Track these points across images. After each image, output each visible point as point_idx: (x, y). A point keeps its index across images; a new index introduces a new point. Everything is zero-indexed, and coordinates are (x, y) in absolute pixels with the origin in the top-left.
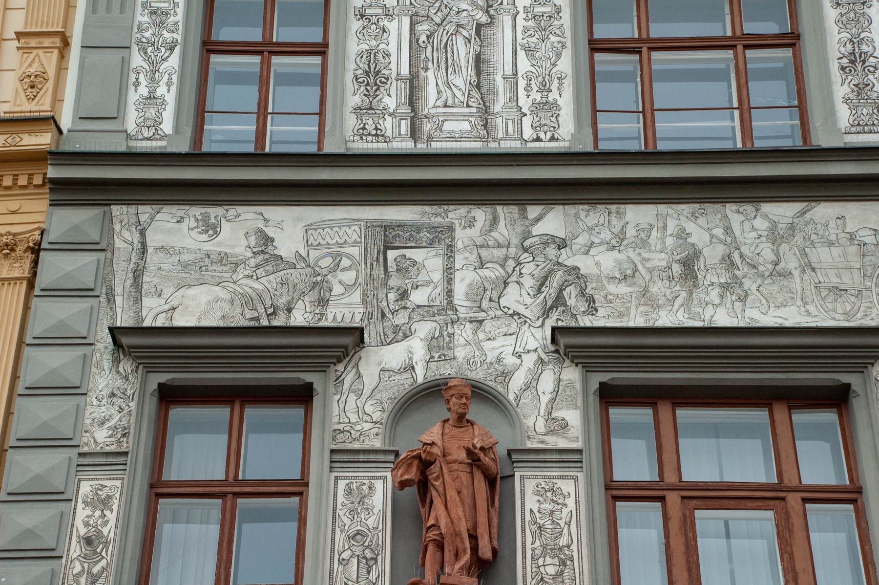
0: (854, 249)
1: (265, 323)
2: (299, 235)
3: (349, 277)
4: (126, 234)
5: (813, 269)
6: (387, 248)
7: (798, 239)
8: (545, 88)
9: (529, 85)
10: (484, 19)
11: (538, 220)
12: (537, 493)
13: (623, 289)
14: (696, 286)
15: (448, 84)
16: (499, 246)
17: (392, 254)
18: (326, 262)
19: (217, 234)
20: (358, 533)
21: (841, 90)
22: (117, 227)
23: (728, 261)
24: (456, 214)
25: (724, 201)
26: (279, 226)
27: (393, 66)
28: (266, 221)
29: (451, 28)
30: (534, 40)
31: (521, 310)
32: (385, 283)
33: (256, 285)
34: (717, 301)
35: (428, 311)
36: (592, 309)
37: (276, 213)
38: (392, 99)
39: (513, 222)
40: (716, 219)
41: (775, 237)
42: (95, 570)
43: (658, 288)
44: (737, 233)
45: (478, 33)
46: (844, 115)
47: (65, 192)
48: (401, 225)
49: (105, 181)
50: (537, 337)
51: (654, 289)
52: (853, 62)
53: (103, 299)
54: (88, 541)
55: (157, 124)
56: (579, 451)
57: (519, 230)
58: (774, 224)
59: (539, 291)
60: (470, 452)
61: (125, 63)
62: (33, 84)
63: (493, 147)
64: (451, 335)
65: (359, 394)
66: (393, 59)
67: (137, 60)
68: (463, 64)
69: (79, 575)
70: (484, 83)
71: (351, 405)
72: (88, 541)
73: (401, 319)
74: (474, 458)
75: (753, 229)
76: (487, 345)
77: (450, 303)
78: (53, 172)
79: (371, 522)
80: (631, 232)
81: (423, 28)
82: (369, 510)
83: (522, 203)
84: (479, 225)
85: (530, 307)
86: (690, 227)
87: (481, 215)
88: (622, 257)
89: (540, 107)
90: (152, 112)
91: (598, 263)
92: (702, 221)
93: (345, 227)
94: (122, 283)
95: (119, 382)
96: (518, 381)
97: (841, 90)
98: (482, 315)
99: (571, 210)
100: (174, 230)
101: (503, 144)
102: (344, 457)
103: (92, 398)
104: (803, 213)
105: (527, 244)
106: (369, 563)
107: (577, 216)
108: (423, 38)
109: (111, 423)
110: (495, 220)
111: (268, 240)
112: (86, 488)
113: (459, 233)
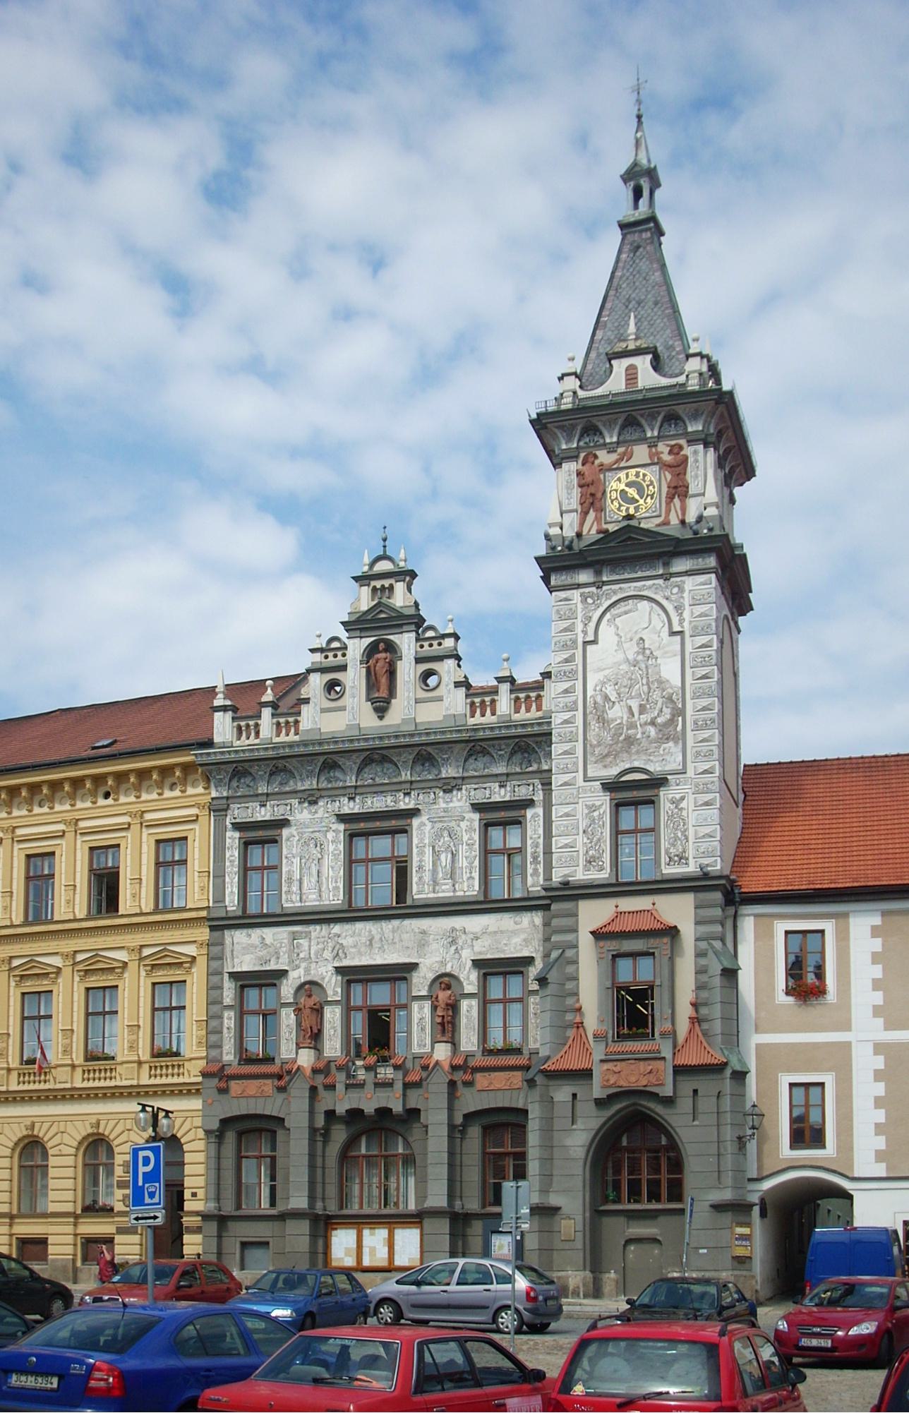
13: (353, 950)
21: (415, 879)
24: (311, 928)
38: (295, 888)
49: (220, 924)
67: (227, 879)
87: (318, 927)
93: (283, 932)
94: (228, 954)
100: (238, 938)
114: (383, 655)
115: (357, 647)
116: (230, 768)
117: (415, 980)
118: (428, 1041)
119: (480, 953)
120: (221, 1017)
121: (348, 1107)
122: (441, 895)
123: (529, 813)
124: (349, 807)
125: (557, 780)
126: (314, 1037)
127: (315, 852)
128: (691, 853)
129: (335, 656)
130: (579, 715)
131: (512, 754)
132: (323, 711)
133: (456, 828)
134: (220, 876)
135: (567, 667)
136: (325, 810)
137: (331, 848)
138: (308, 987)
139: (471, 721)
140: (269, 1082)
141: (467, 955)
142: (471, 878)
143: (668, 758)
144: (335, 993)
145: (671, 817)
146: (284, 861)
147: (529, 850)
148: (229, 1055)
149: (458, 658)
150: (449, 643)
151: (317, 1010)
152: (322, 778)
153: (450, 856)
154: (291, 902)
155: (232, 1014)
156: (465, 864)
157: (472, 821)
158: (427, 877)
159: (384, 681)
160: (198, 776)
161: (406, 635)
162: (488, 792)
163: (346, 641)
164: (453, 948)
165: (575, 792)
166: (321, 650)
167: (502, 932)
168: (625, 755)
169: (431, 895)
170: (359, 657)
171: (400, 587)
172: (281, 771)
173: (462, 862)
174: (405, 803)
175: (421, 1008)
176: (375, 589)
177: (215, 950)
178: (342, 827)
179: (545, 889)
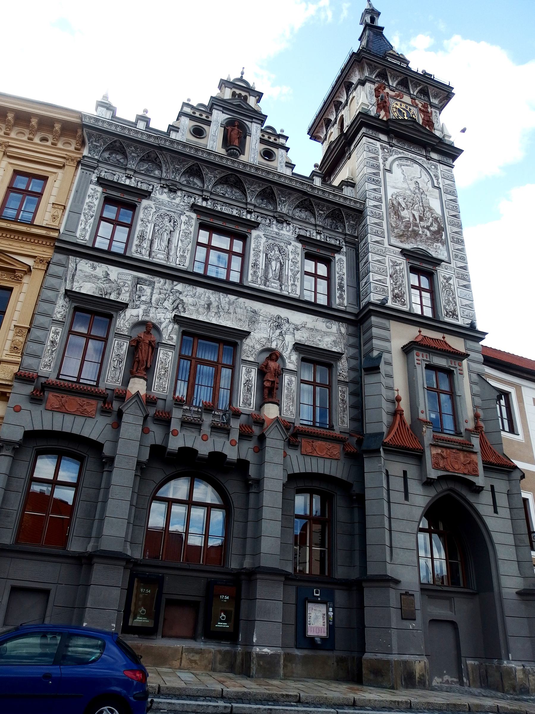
1: (104, 297)
2: (116, 275)
4: (72, 264)
6: (138, 284)
7: (234, 305)
8: (184, 252)
13: (192, 308)
14: (209, 311)
17: (138, 286)
21: (251, 272)
22: (70, 262)
23: (218, 306)
24: (156, 279)
25: (220, 292)
26: (111, 271)
27: (147, 236)
29: (164, 230)
31: (168, 307)
33: (103, 286)
35: (145, 302)
36: (184, 312)
37: (111, 268)
38: (146, 244)
39: (170, 284)
41: (230, 303)
42: (53, 349)
43: (201, 310)
45: (170, 233)
46: (250, 278)
47: (58, 250)
48: (142, 278)
50: (170, 315)
51: (200, 310)
54: (52, 342)
55: (84, 236)
56: (175, 346)
60: (149, 341)
61: (79, 218)
62: (54, 218)
63: (168, 264)
66: (148, 234)
67: (82, 217)
69: (49, 350)
71: (122, 322)
72: (52, 342)
73: (138, 303)
74: (150, 343)
78: (56, 244)
80: (197, 294)
81: (157, 228)
82: (122, 349)
83: (173, 281)
85: (170, 308)
87: (162, 281)
89: (182, 256)
91: (188, 300)
92: (214, 295)
93: (128, 275)
94: (69, 277)
95: (65, 303)
96: (163, 326)
99: (184, 285)
100: (85, 266)
101: (171, 264)
103: (57, 306)
107: (185, 287)
110: (165, 283)
111: (108, 274)
112: (53, 328)
113: (156, 284)
115: (219, 117)
116: (110, 140)
117: (245, 347)
118: (253, 401)
120: (46, 329)
121: (181, 444)
127: (169, 226)
128: (459, 312)
130: (383, 205)
133: (284, 248)
136: (179, 200)
137: (183, 227)
141: (290, 340)
143: (439, 251)
145: (444, 286)
147: (337, 281)
150: (281, 141)
152: (183, 179)
153: (278, 265)
156: (290, 274)
157: (296, 247)
158: (260, 273)
161: (254, 125)
164: (278, 331)
168: (413, 240)
175: (249, 372)
178: (194, 216)
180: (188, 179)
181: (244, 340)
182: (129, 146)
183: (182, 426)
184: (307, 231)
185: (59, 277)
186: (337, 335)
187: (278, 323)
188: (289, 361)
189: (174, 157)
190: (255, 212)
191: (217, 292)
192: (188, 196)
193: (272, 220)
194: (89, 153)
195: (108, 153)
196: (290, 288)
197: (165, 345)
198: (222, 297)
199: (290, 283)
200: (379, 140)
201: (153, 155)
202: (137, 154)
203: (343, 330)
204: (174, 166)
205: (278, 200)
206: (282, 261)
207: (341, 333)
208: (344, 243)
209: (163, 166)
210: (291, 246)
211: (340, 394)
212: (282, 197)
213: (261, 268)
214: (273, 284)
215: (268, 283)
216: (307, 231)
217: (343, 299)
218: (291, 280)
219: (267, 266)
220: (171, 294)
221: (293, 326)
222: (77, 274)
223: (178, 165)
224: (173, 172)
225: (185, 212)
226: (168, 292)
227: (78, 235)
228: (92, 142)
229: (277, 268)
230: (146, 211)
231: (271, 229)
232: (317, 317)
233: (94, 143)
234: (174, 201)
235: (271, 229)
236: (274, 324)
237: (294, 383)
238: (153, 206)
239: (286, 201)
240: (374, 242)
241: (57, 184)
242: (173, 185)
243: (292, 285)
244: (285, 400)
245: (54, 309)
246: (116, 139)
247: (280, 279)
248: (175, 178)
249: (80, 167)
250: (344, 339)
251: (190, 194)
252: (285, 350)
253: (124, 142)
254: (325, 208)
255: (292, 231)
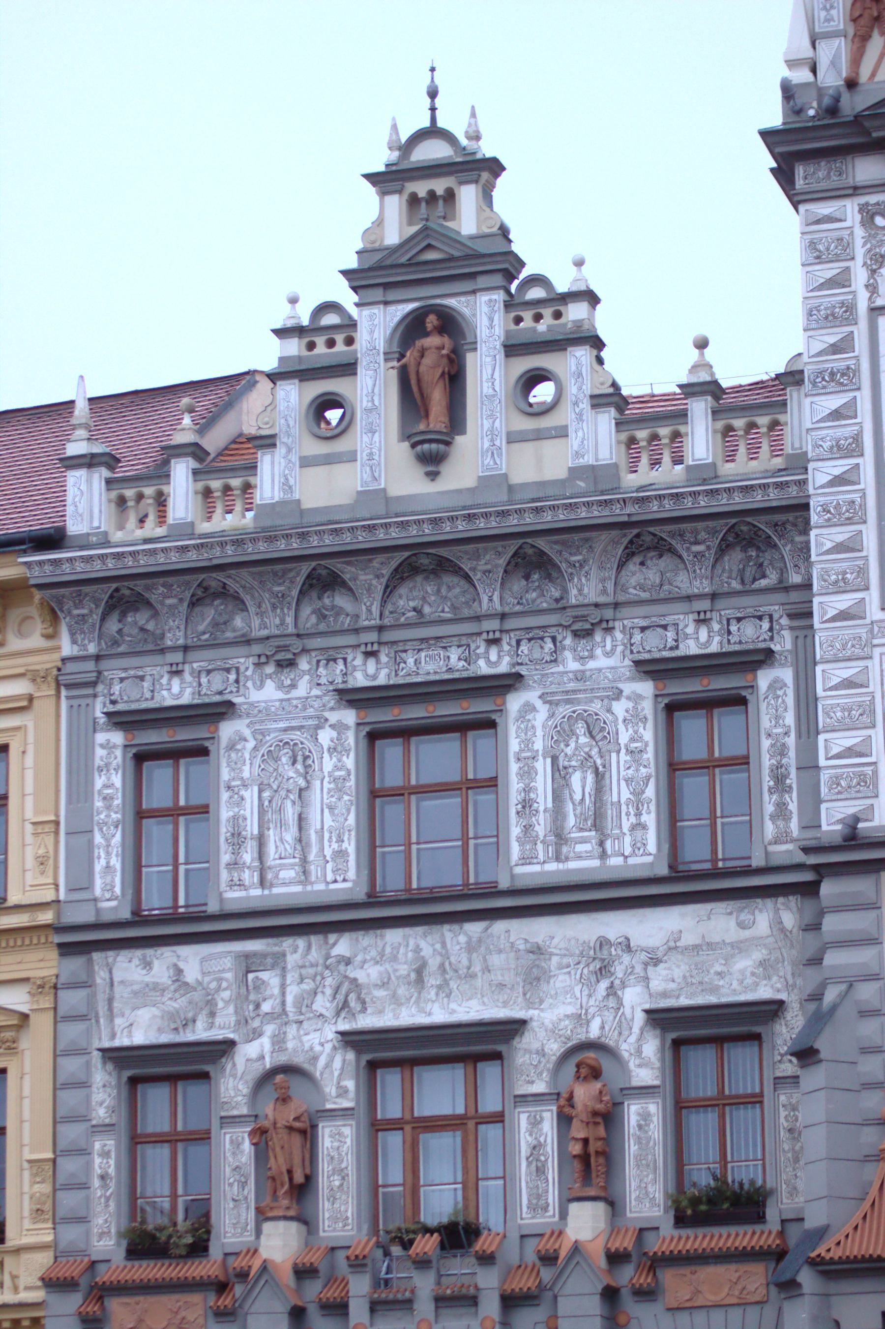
0: (512, 955)
2: (197, 967)
3: (226, 994)
4: (102, 973)
5: (489, 971)
6: (248, 972)
9: (330, 837)
10: (302, 783)
11: (334, 944)
12: (331, 1136)
13: (381, 993)
14: (423, 988)
15: (281, 840)
16: (312, 966)
17: (251, 976)
18: (213, 985)
19: (151, 969)
20: (237, 1167)
21: (515, 831)
22: (96, 968)
23: (442, 968)
24: (287, 943)
26: (186, 961)
27: (248, 828)
28: (179, 957)
29: (283, 793)
30: (333, 799)
31: (324, 1012)
32: (247, 998)
33: (176, 1005)
34: (434, 998)
35: (271, 1017)
36: (364, 1010)
37: (185, 951)
38: (248, 856)
39: (320, 947)
40: (437, 936)
42: (108, 1194)
43: (402, 991)
44: (449, 946)
45: (300, 796)
47: (66, 950)
48: (255, 954)
50: (330, 1033)
52: (524, 807)
53: (93, 1021)
56: (353, 1109)
57: (324, 952)
58: (470, 938)
59: (334, 998)
61: (91, 842)
64: (285, 1033)
65: (234, 1076)
66: (249, 822)
67: (98, 839)
68: (291, 822)
69: (100, 1197)
70: (304, 838)
71: (231, 1085)
73: (256, 1023)
75: (458, 943)
76: (305, 1038)
77: (284, 1010)
79: (244, 1160)
80: (388, 950)
81: (266, 794)
82: (242, 1152)
84: (300, 950)
86: (423, 944)
87: (301, 942)
88: (382, 969)
90: (108, 890)
91: (368, 974)
92: (429, 938)
94: (102, 1009)
97: (515, 831)
98: (302, 1018)
99: (354, 935)
100: (127, 968)
102: (228, 1121)
103: (94, 1089)
104: (487, 929)
105: (328, 963)
106: (243, 1185)
107: (357, 940)
108: (266, 803)
109: (105, 1104)
110: (309, 947)
111: (179, 971)
112: (97, 1146)
114: (433, 341)
115: (377, 326)
116: (104, 592)
118: (553, 1197)
119: (665, 995)
120: (84, 1152)
122: (573, 865)
123: (764, 679)
124: (366, 673)
125: (826, 605)
126: (292, 1191)
127: (292, 774)
129: (331, 343)
131: (724, 549)
132: (306, 462)
133: (604, 715)
134: (81, 831)
135: (838, 362)
136: (307, 685)
137: (328, 764)
138: (283, 1077)
139: (631, 480)
140: (196, 1298)
141: (635, 1001)
142: (639, 826)
144: (343, 1092)
146: (225, 796)
147: (767, 762)
148: (104, 1237)
149: (598, 344)
150: (576, 312)
151: (303, 1132)
152: (306, 610)
153: (590, 778)
154: (239, 891)
155: (111, 1143)
156: (626, 794)
157: (636, 698)
158: (541, 827)
159: (437, 397)
160: (33, 611)
162: (670, 635)
163: (354, 311)
164: (603, 985)
165: (863, 632)
166: (298, 331)
167: (711, 946)
169: (552, 866)
170: (381, 346)
171: (468, 196)
172: (216, 595)
173: (619, 792)
174: (492, 662)
175: (535, 1123)
176: (414, 201)
177: (71, 999)
178: (349, 717)
179: (806, 850)
180: (319, 604)
181: (517, 1039)
182: (148, 588)
183: (372, 1310)
184: (665, 627)
185: (83, 1018)
186: (771, 939)
187: (601, 963)
188: (637, 1062)
189: (260, 574)
190: (507, 631)
191: (435, 928)
192: (328, 661)
193: (559, 638)
194: (74, 642)
195: (115, 616)
196: (628, 839)
197: (332, 1114)
198: (448, 935)
199: (625, 829)
200: (856, 190)
201: (213, 584)
202: (176, 596)
203: (789, 919)
204: (270, 590)
205: (563, 566)
206: (599, 762)
207: (783, 930)
208: (785, 621)
209: (247, 599)
210: (623, 700)
211: (783, 1113)
212: (571, 554)
213: (542, 808)
214: (580, 848)
215: (565, 849)
216: (665, 627)
217: (787, 818)
218: (628, 814)
219: (557, 797)
220: (327, 973)
221: (643, 956)
222: (117, 996)
223: (280, 585)
224: (274, 607)
225: (327, 714)
226: (320, 968)
227: (98, 892)
228: (69, 612)
229: (587, 790)
230: (233, 755)
231: (561, 668)
232: (708, 906)
233: (76, 612)
234: (295, 693)
235: (561, 668)
236: (591, 968)
237: (655, 1119)
238: (247, 733)
239: (585, 561)
240: (833, 619)
241: (29, 761)
242: (280, 649)
243: (633, 828)
244: (633, 1172)
245: (88, 1098)
246: (114, 586)
247: (597, 821)
248: (283, 622)
249: (64, 693)
250: (792, 945)
251: (331, 652)
252: (626, 1033)
253: (135, 585)
254: (703, 535)
255: (620, 649)
